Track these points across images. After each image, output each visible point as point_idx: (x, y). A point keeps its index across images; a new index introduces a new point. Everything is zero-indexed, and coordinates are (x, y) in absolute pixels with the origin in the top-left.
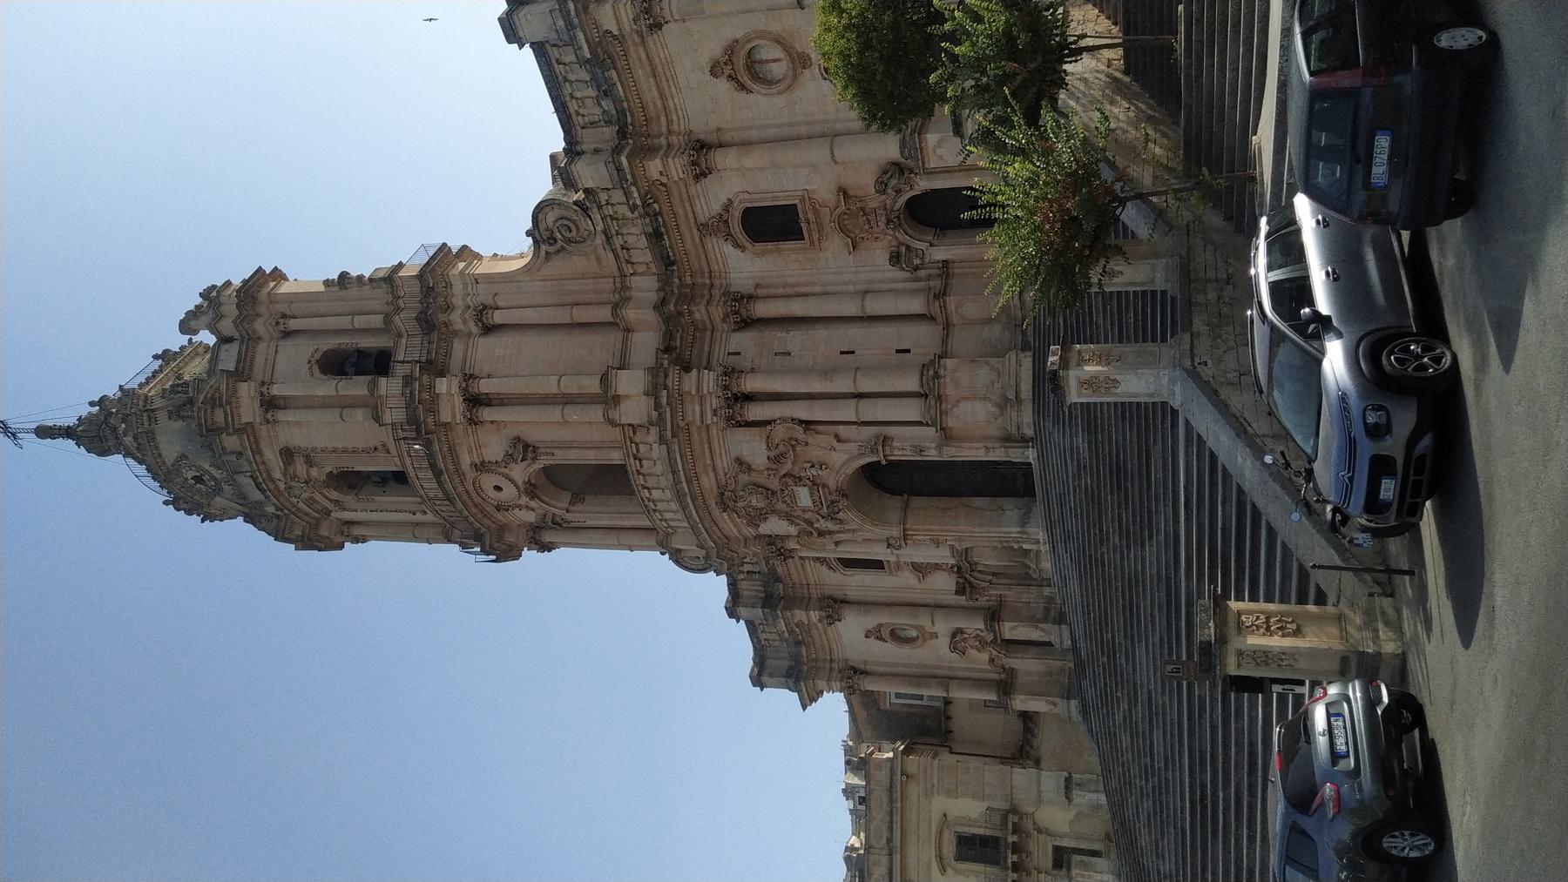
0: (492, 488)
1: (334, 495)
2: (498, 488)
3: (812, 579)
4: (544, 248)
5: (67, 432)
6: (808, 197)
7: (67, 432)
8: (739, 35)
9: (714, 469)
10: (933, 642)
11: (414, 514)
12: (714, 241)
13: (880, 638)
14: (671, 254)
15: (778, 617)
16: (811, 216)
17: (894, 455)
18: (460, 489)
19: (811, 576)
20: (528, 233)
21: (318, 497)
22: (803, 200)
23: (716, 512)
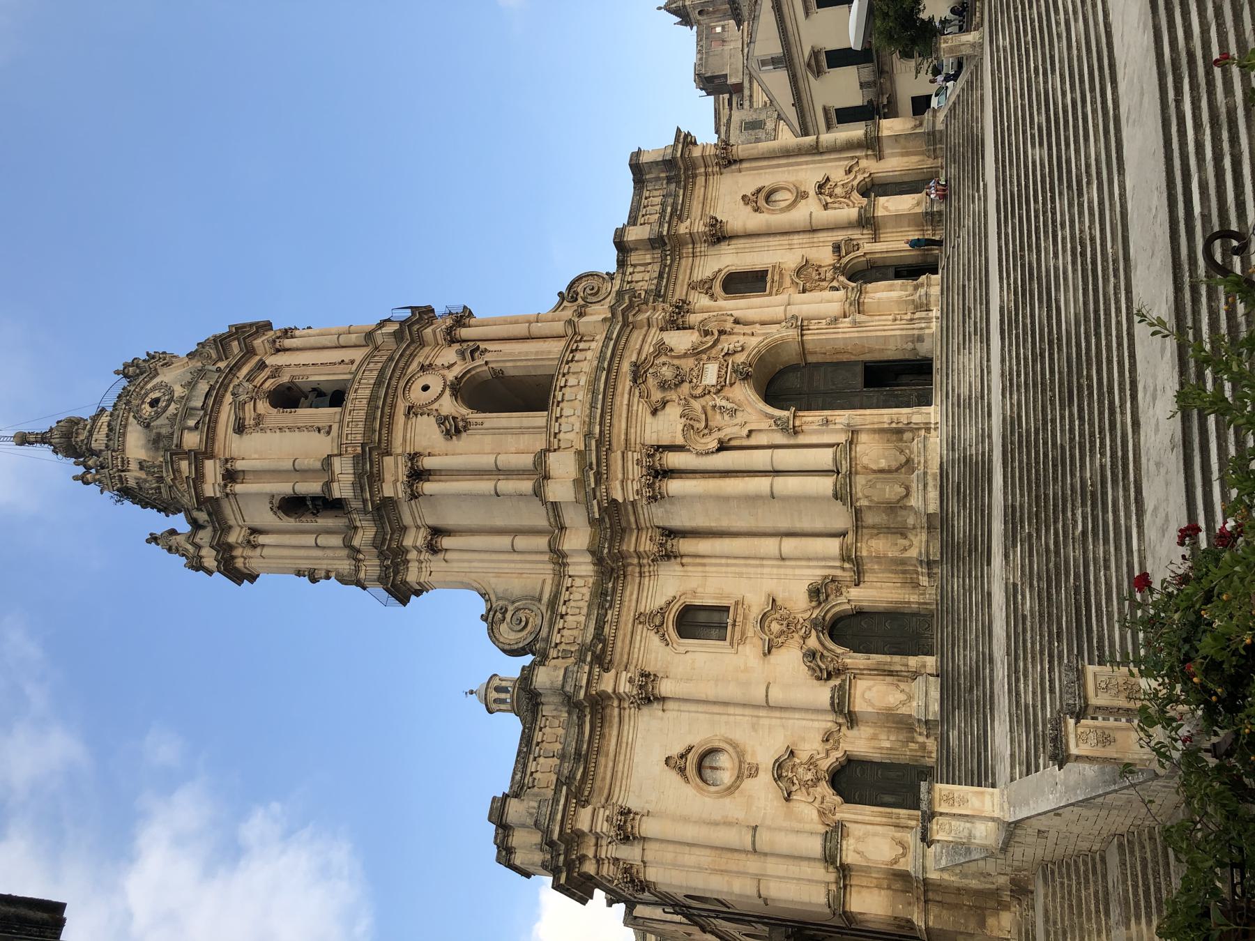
0: (427, 383)
1: (263, 406)
2: (425, 388)
3: (636, 656)
4: (565, 303)
5: (43, 439)
6: (778, 268)
7: (43, 439)
8: (766, 185)
9: (639, 354)
10: (748, 784)
11: (319, 431)
12: (697, 294)
13: (682, 771)
14: (662, 291)
15: (584, 661)
16: (776, 278)
17: (809, 329)
18: (394, 382)
19: (636, 650)
20: (560, 294)
21: (249, 407)
22: (774, 267)
23: (625, 383)
